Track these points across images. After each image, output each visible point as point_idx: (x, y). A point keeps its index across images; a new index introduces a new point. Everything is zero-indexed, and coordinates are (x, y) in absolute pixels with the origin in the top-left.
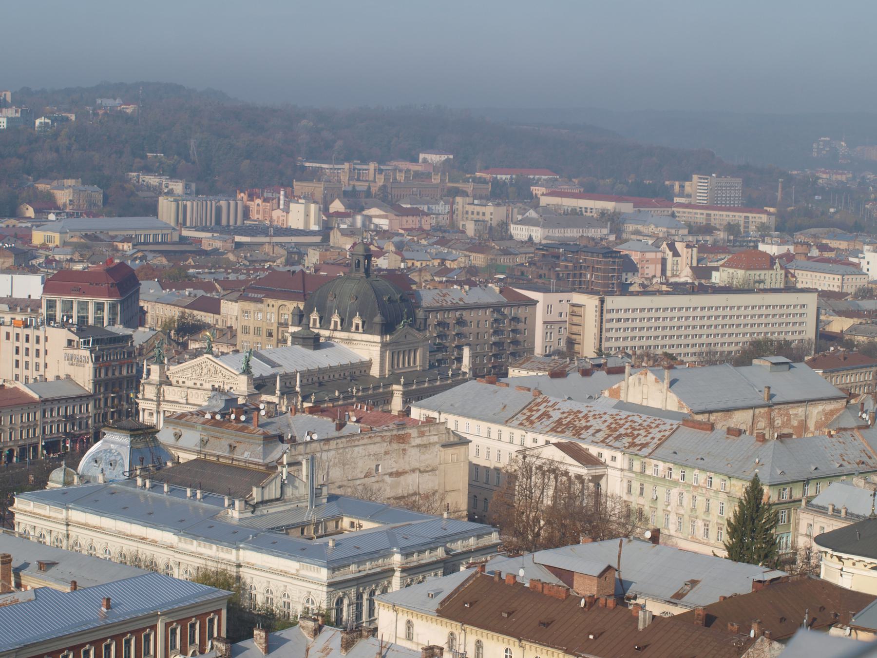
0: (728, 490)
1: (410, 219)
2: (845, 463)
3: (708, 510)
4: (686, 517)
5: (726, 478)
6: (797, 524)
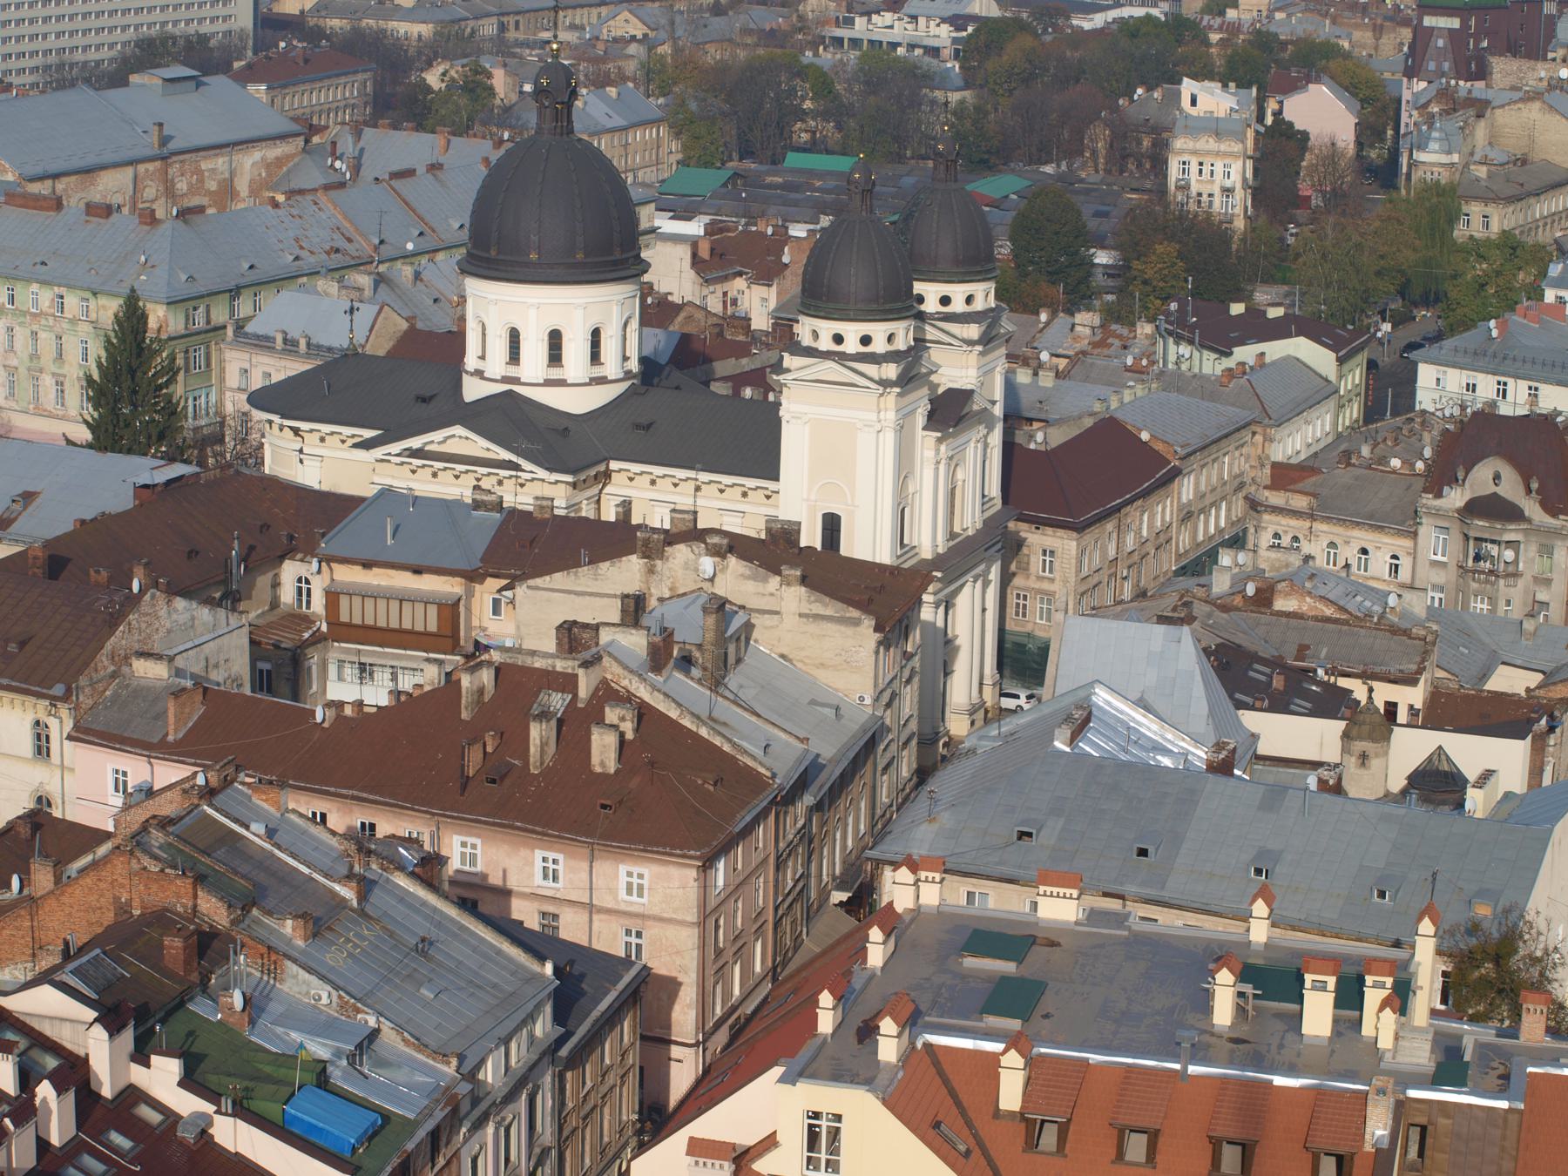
0: (93, 316)
2: (305, 254)
3: (60, 355)
4: (22, 371)
5: (88, 295)
6: (223, 370)
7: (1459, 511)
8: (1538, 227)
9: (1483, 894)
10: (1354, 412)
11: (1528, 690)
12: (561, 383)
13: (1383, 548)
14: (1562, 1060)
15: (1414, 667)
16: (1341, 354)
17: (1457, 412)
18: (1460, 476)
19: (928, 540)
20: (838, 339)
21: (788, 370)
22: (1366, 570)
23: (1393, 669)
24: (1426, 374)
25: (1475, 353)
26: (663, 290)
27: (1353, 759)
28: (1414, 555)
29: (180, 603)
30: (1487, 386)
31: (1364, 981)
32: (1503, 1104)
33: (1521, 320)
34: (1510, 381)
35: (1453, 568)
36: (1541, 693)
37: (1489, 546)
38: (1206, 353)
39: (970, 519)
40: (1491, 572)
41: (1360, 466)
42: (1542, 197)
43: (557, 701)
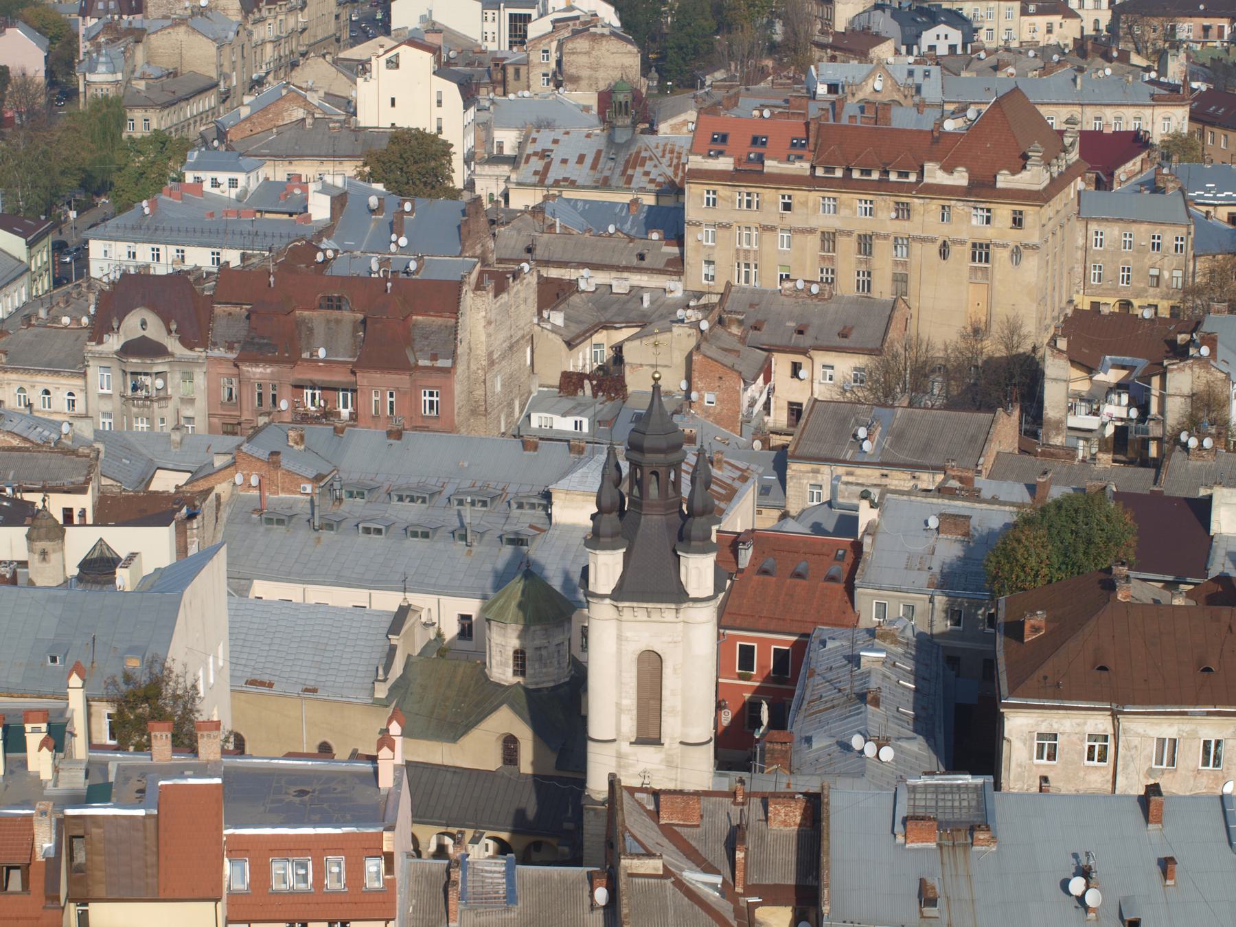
7: (117, 353)
8: (189, 125)
9: (133, 650)
10: (44, 284)
11: (177, 487)
13: (61, 386)
14: (187, 773)
15: (82, 479)
16: (29, 239)
18: (115, 325)
22: (50, 407)
23: (66, 482)
24: (96, 248)
25: (133, 228)
27: (36, 556)
28: (86, 391)
30: (144, 253)
31: (24, 728)
32: (141, 812)
33: (167, 198)
34: (162, 247)
35: (117, 398)
36: (188, 488)
37: (143, 378)
40: (147, 398)
41: (39, 326)
42: (191, 101)
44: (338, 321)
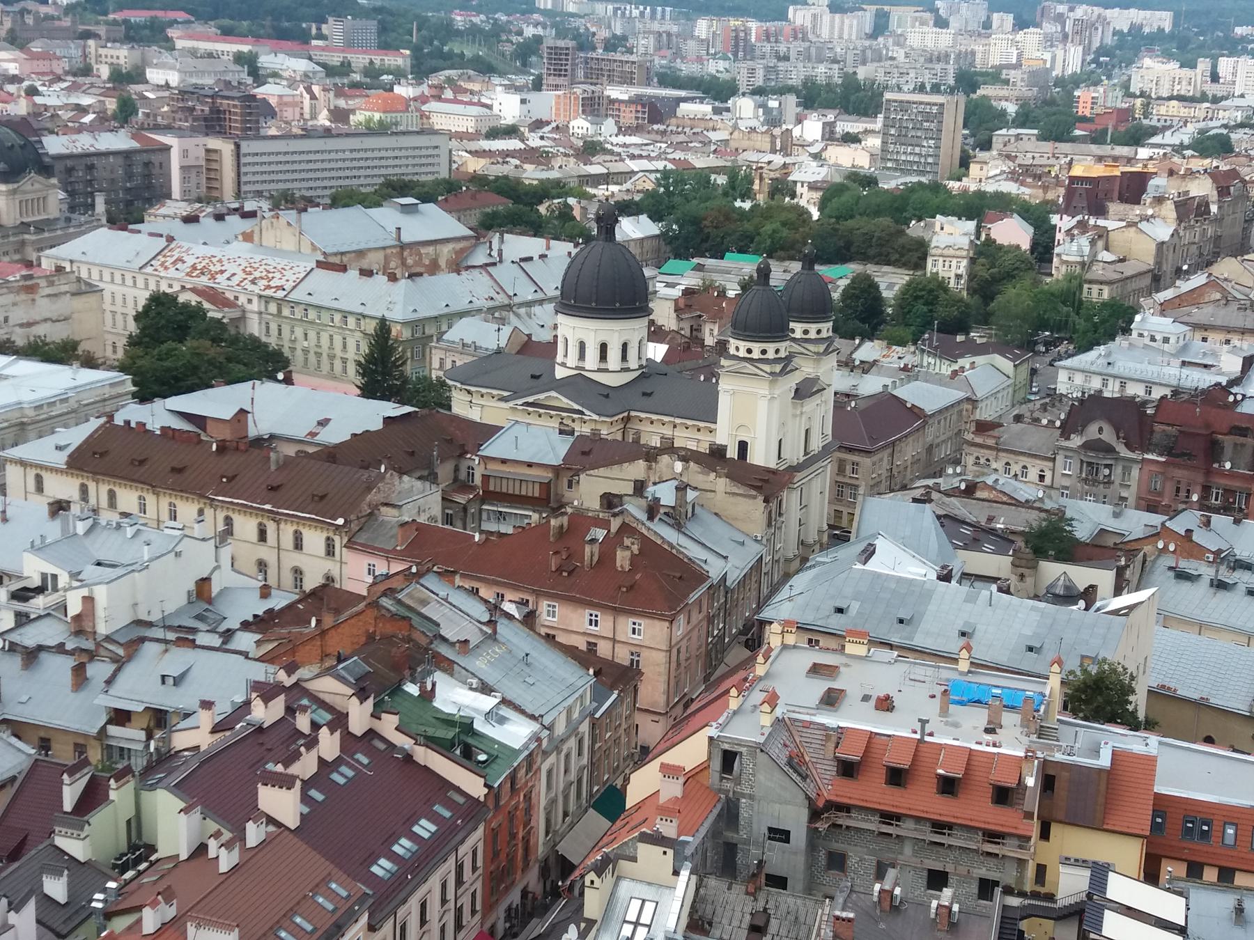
0: (362, 328)
1: (41, 62)
2: (474, 299)
3: (345, 346)
4: (325, 355)
6: (431, 358)
12: (606, 370)
17: (1080, 395)
19: (794, 454)
20: (749, 351)
21: (723, 367)
26: (660, 323)
29: (405, 478)
35: (1074, 476)
38: (943, 361)
39: (816, 445)
43: (600, 534)
44: (1243, 445)
